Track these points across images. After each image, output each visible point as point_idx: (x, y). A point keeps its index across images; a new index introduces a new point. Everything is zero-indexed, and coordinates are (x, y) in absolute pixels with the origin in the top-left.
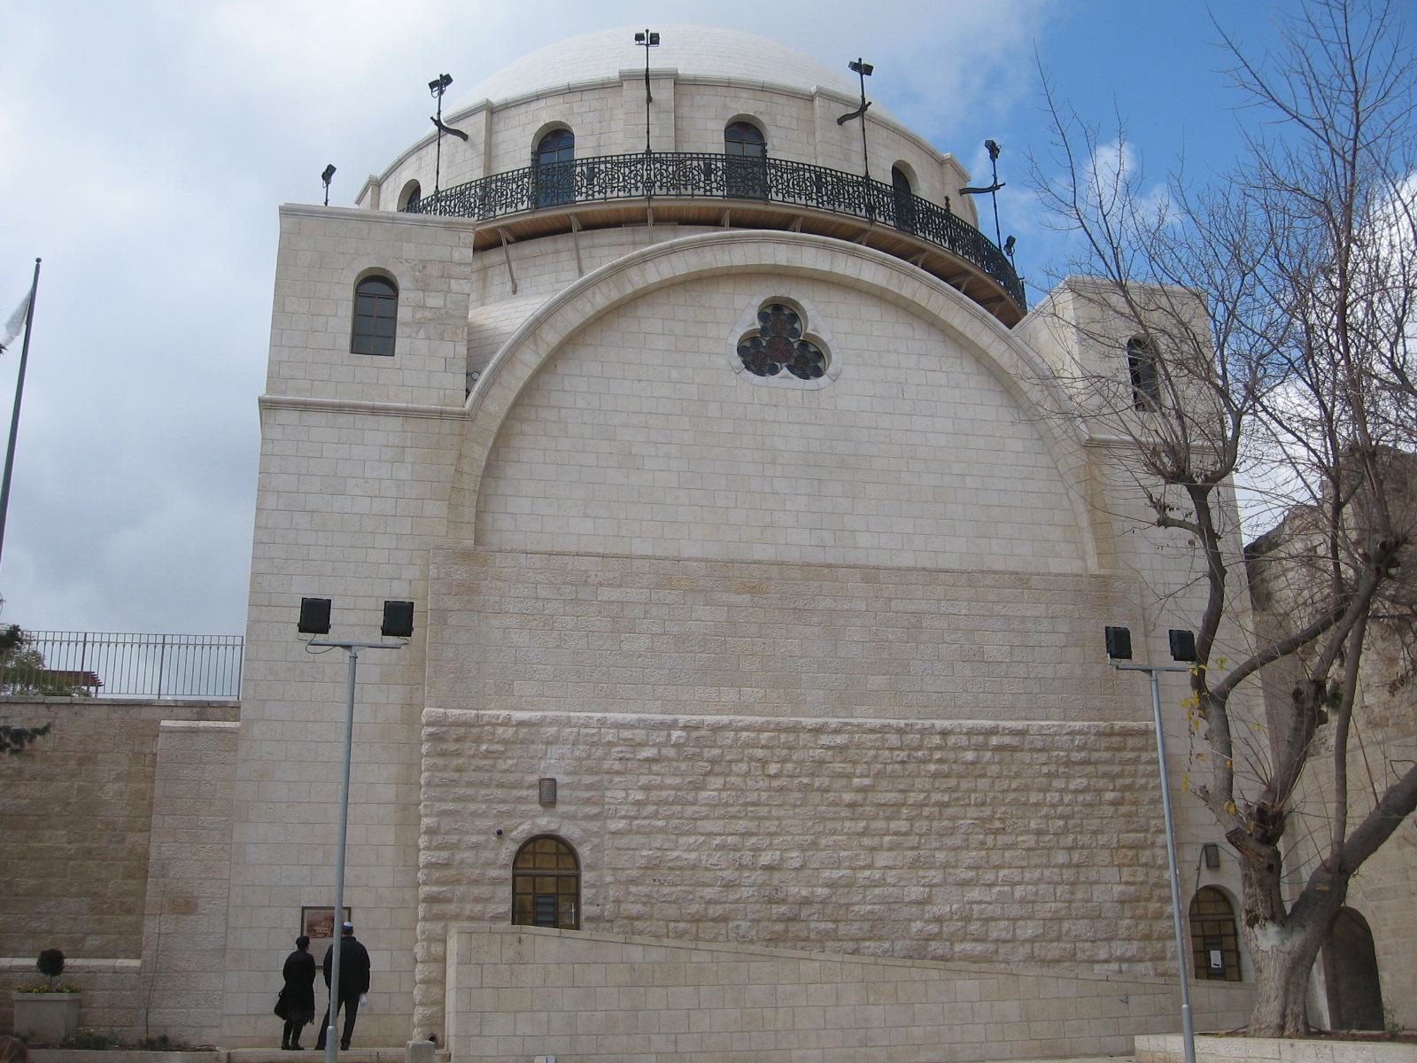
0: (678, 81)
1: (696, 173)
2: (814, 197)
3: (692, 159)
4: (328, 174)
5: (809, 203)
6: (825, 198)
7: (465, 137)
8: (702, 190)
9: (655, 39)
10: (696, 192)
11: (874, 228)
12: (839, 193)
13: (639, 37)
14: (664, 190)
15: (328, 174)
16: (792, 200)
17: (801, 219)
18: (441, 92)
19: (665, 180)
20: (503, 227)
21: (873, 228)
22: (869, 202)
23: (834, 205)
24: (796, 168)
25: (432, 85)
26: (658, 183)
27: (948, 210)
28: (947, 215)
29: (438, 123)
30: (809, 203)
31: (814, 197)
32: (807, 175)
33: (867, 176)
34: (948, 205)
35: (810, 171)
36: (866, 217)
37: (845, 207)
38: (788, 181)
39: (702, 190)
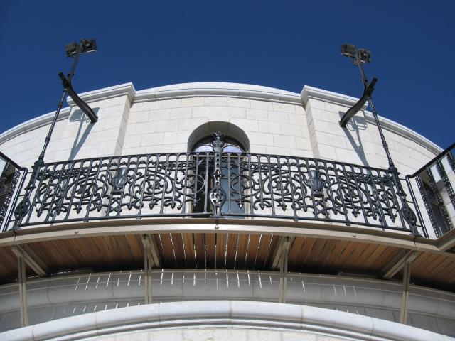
1: (100, 184)
2: (309, 202)
5: (301, 213)
6: (329, 204)
8: (104, 209)
12: (351, 194)
14: (45, 213)
16: (268, 211)
17: (287, 245)
19: (49, 200)
23: (345, 214)
24: (271, 167)
26: (38, 206)
30: (301, 213)
31: (309, 202)
36: (404, 229)
37: (366, 215)
38: (262, 182)
39: (104, 209)
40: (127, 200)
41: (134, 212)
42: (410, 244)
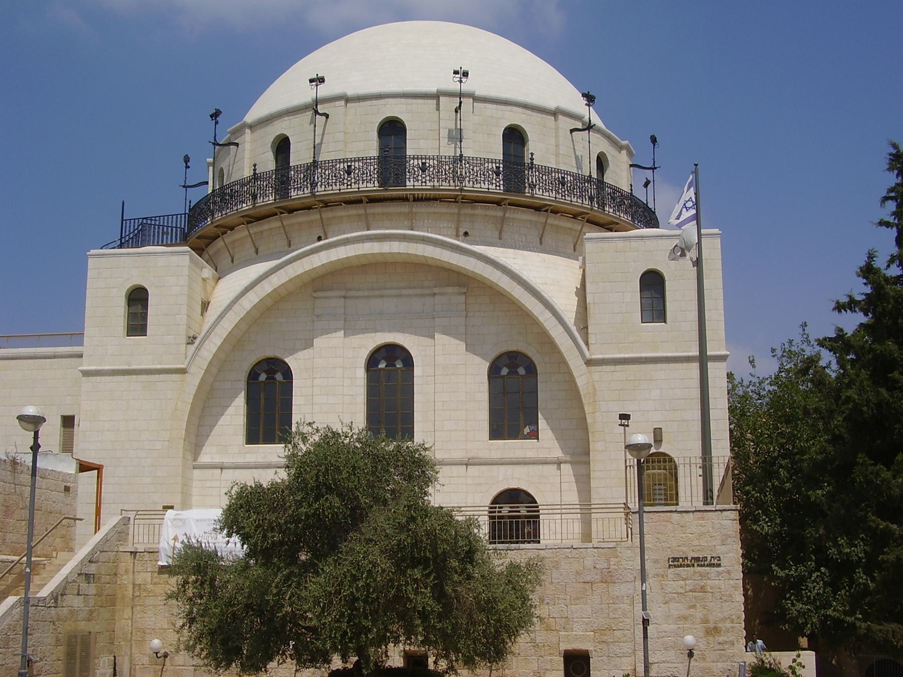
0: (347, 99)
3: (340, 162)
4: (187, 160)
6: (428, 178)
7: (237, 145)
9: (321, 80)
10: (342, 187)
13: (311, 81)
15: (187, 160)
18: (216, 123)
20: (243, 217)
25: (211, 116)
27: (532, 163)
28: (532, 166)
29: (215, 144)
32: (416, 163)
33: (461, 156)
34: (532, 159)
35: (418, 159)
40: (353, 181)
41: (357, 186)
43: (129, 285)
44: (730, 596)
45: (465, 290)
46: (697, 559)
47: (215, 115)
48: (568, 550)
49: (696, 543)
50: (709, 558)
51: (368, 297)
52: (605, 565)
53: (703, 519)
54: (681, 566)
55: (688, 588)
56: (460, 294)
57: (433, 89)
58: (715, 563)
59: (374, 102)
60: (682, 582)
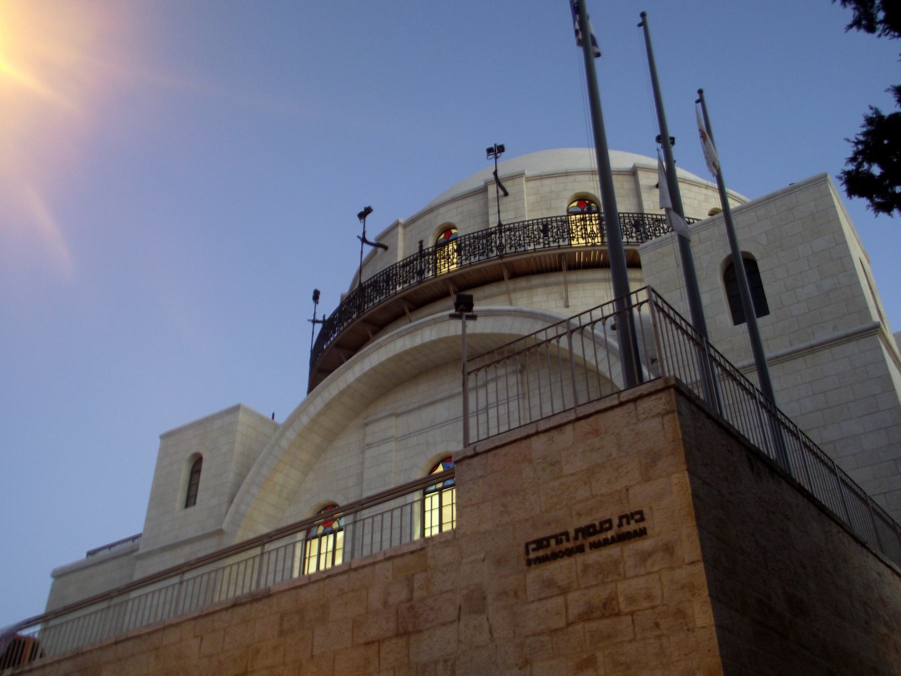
11: (504, 260)
21: (504, 260)
22: (501, 243)
42: (500, 261)
43: (188, 455)
44: (680, 613)
45: (519, 367)
46: (587, 531)
47: (316, 296)
48: (345, 577)
49: (582, 493)
50: (616, 522)
51: (420, 408)
52: (404, 594)
53: (596, 432)
54: (555, 556)
55: (574, 611)
56: (514, 372)
57: (482, 184)
58: (630, 528)
59: (427, 218)
60: (560, 600)
